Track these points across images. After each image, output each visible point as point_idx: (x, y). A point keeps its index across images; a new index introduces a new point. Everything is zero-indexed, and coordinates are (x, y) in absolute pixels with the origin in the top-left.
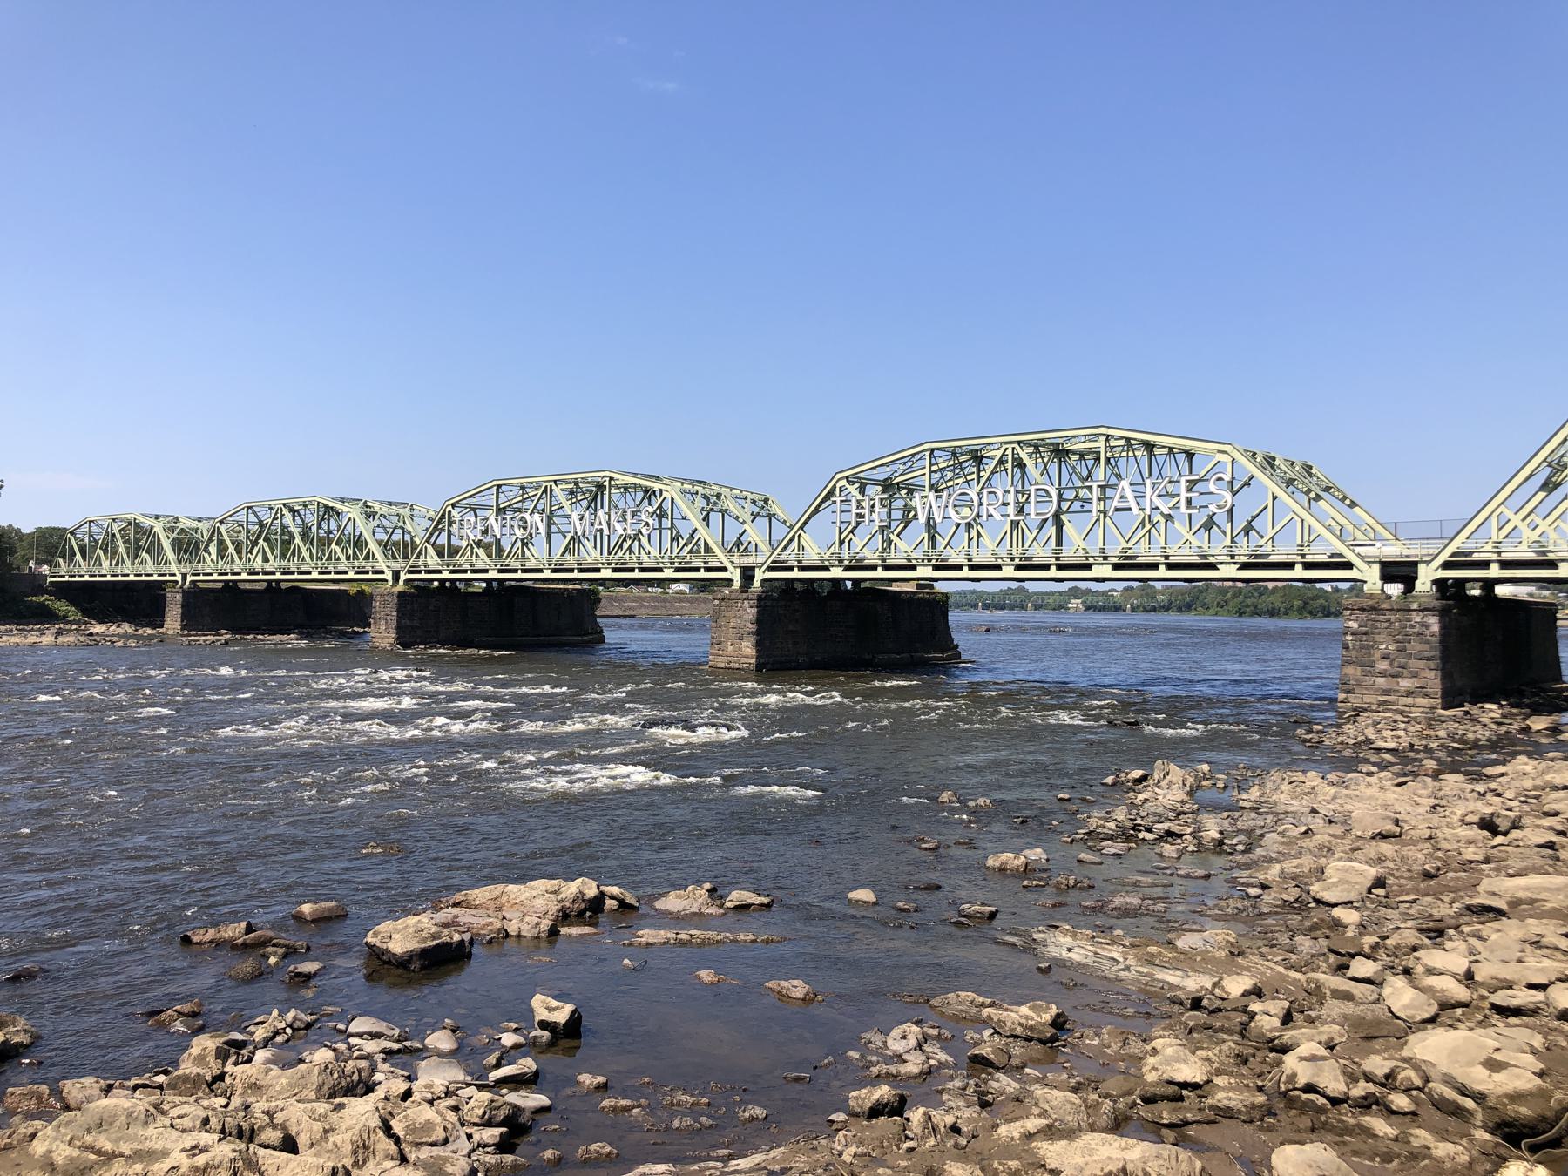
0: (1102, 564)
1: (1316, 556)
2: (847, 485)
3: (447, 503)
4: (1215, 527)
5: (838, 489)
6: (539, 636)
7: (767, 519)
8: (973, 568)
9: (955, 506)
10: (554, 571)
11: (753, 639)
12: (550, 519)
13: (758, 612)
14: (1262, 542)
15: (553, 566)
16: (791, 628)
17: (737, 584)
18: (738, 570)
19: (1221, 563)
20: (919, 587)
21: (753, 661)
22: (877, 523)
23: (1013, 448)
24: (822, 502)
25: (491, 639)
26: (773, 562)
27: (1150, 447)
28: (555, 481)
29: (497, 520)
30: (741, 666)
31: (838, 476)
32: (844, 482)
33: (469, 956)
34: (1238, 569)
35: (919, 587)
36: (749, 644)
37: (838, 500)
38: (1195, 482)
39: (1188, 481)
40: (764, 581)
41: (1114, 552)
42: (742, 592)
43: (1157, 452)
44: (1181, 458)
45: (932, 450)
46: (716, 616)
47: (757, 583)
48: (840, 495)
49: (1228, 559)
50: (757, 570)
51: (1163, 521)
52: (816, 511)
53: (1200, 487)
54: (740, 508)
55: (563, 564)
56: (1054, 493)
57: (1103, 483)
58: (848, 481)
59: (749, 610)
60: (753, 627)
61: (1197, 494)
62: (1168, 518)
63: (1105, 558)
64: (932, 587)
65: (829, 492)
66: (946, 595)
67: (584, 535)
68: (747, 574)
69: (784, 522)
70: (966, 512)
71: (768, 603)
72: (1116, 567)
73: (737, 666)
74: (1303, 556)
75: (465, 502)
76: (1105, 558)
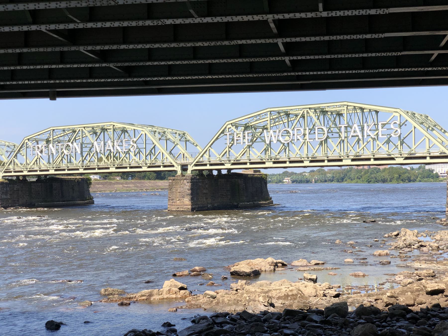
0: (347, 159)
1: (435, 154)
2: (232, 127)
3: (25, 139)
4: (391, 142)
5: (227, 129)
6: (64, 201)
7: (185, 143)
8: (329, 161)
9: (282, 136)
10: (85, 169)
11: (189, 197)
12: (82, 145)
13: (191, 185)
15: (84, 167)
16: (205, 191)
17: (179, 172)
18: (180, 166)
19: (397, 157)
20: (255, 171)
21: (190, 207)
22: (247, 144)
23: (307, 111)
24: (220, 135)
25: (43, 203)
26: (197, 162)
27: (362, 109)
28: (84, 127)
29: (53, 146)
30: (184, 210)
31: (227, 123)
32: (230, 126)
33: (260, 274)
34: (404, 160)
35: (255, 171)
36: (187, 200)
37: (228, 134)
38: (385, 124)
39: (382, 124)
40: (192, 171)
41: (352, 154)
42: (182, 176)
43: (365, 111)
44: (374, 113)
45: (271, 111)
46: (170, 188)
47: (189, 172)
48: (229, 132)
49: (399, 156)
50: (189, 166)
51: (372, 140)
52: (217, 138)
53: (387, 126)
54: (174, 137)
55: (122, 165)
56: (326, 130)
57: (347, 125)
58: (232, 125)
59: (187, 184)
60: (190, 192)
61: (386, 129)
62: (374, 139)
63: (348, 157)
64: (259, 171)
65: (223, 130)
66: (266, 175)
67: (100, 152)
68: (184, 168)
69: (194, 144)
70: (287, 138)
71: (195, 181)
72: (353, 160)
73: (182, 209)
74: (430, 154)
75: (34, 138)
76: (348, 157)
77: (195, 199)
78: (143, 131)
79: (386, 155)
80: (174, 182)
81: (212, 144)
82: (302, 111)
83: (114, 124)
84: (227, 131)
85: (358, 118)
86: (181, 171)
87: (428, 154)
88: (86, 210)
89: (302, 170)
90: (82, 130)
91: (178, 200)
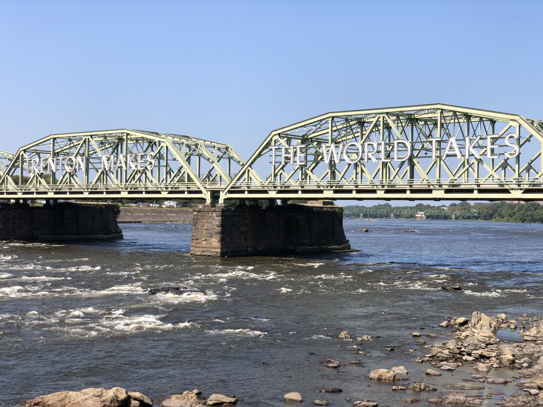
0: (438, 190)
2: (279, 139)
3: (21, 149)
4: (508, 167)
5: (273, 142)
6: (80, 234)
8: (358, 191)
9: (347, 153)
10: (91, 193)
11: (218, 237)
12: (88, 160)
13: (222, 220)
14: (537, 176)
15: (90, 190)
16: (243, 229)
17: (209, 201)
18: (209, 193)
19: (512, 189)
20: (324, 203)
21: (219, 250)
22: (298, 163)
23: (384, 117)
24: (263, 149)
25: (48, 237)
27: (468, 117)
28: (91, 136)
29: (53, 161)
30: (211, 254)
31: (274, 133)
32: (277, 137)
34: (522, 193)
36: (216, 240)
37: (273, 148)
39: (492, 138)
40: (226, 200)
41: (446, 182)
42: (212, 207)
43: (472, 119)
44: (488, 123)
45: (333, 118)
46: (195, 222)
47: (221, 201)
48: (275, 145)
49: (517, 187)
50: (221, 192)
51: (476, 163)
52: (260, 155)
53: (499, 142)
54: (210, 153)
55: (96, 189)
56: (409, 145)
57: (439, 139)
58: (280, 137)
59: (216, 218)
60: (219, 229)
61: (497, 146)
62: (480, 161)
63: (440, 186)
64: (332, 204)
65: (268, 143)
66: (341, 209)
67: (110, 170)
68: (215, 195)
69: (239, 162)
70: (354, 156)
71: (228, 214)
72: (447, 191)
73: (208, 254)
75: (32, 148)
76: (440, 186)
77: (228, 239)
78: (163, 142)
79: (497, 186)
80: (199, 214)
81: (252, 162)
82: (377, 118)
83: (128, 132)
84: (273, 145)
85: (461, 129)
86: (210, 199)
87: (517, 186)
88: (108, 248)
89: (377, 203)
90: (89, 139)
91: (204, 240)
